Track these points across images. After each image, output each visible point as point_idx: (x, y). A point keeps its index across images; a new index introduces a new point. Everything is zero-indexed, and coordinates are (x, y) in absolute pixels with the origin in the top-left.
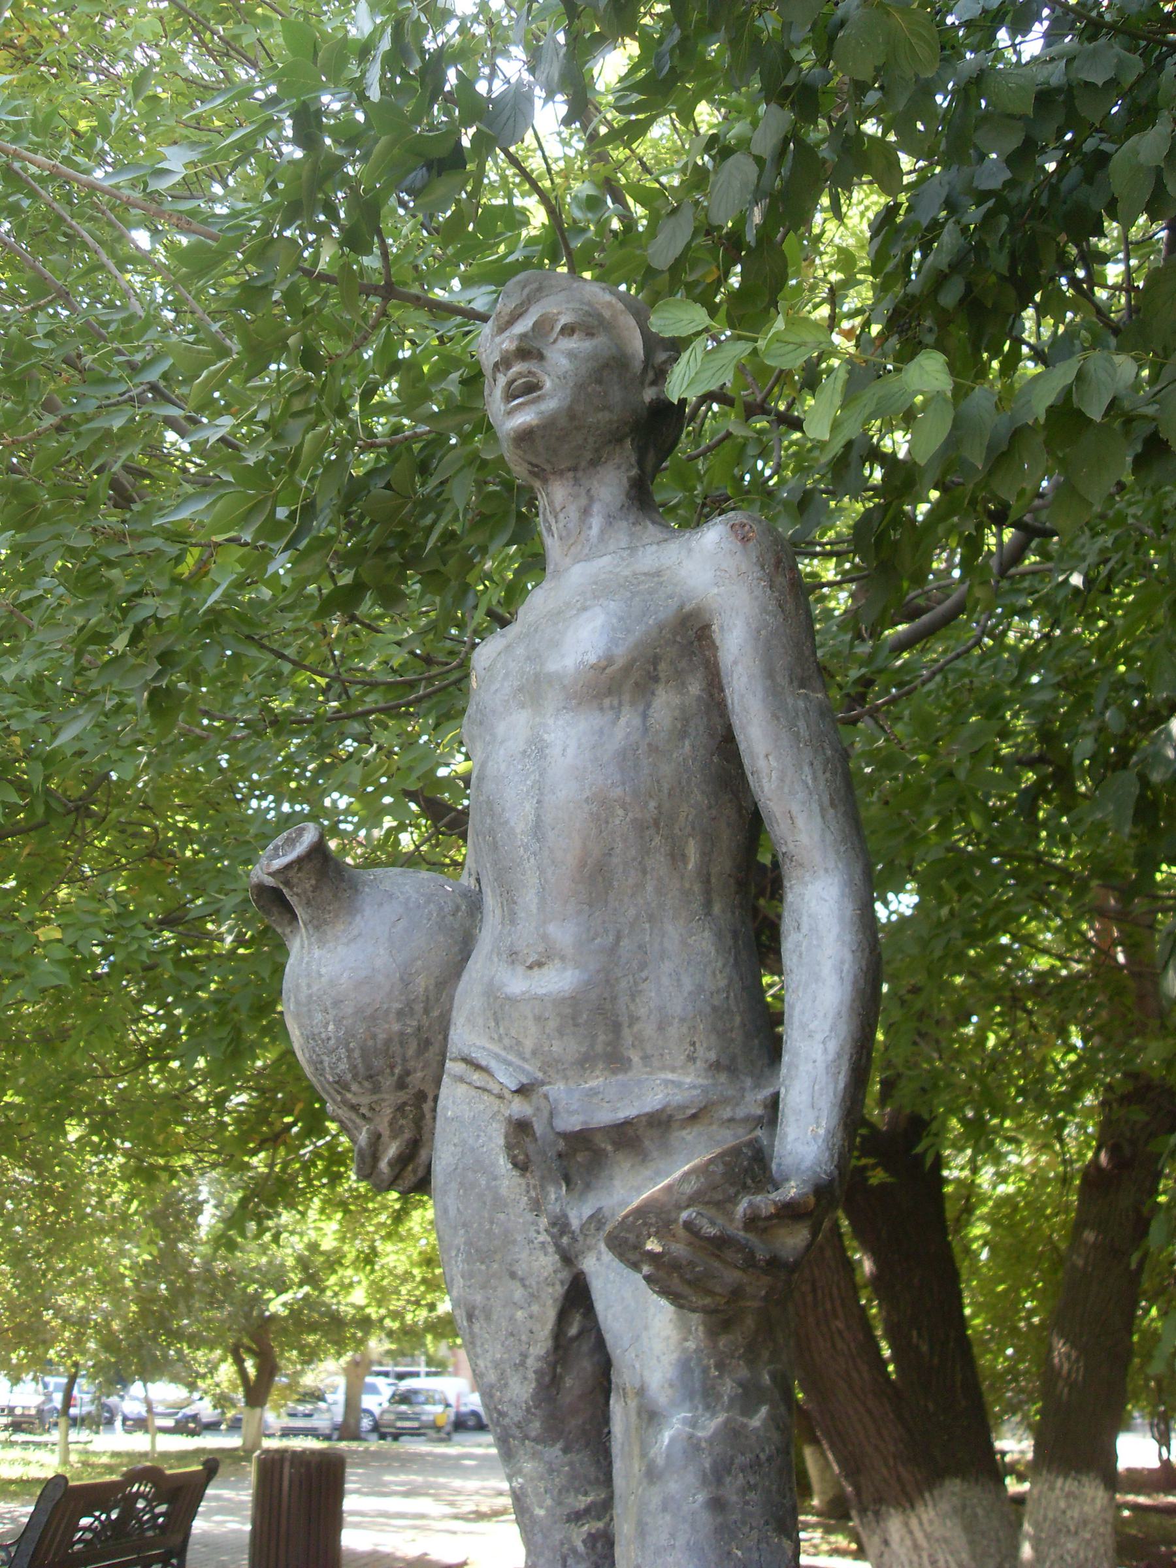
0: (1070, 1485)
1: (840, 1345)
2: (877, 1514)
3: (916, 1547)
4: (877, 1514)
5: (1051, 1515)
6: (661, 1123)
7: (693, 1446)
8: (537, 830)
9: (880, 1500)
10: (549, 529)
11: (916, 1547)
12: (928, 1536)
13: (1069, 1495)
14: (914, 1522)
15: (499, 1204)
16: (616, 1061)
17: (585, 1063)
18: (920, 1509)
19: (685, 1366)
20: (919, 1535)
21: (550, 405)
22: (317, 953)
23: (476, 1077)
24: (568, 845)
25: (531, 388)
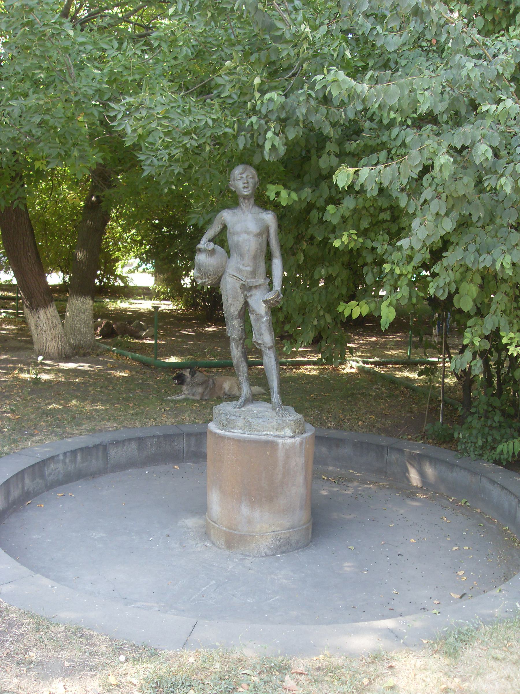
0: (83, 299)
1: (30, 260)
2: (37, 310)
3: (48, 318)
4: (37, 310)
5: (77, 308)
6: (260, 285)
7: (267, 320)
8: (248, 250)
9: (38, 306)
11: (48, 318)
12: (51, 316)
13: (83, 302)
14: (47, 312)
15: (237, 292)
16: (255, 278)
17: (251, 278)
18: (49, 308)
19: (266, 312)
20: (49, 315)
21: (250, 192)
24: (252, 253)
25: (247, 188)
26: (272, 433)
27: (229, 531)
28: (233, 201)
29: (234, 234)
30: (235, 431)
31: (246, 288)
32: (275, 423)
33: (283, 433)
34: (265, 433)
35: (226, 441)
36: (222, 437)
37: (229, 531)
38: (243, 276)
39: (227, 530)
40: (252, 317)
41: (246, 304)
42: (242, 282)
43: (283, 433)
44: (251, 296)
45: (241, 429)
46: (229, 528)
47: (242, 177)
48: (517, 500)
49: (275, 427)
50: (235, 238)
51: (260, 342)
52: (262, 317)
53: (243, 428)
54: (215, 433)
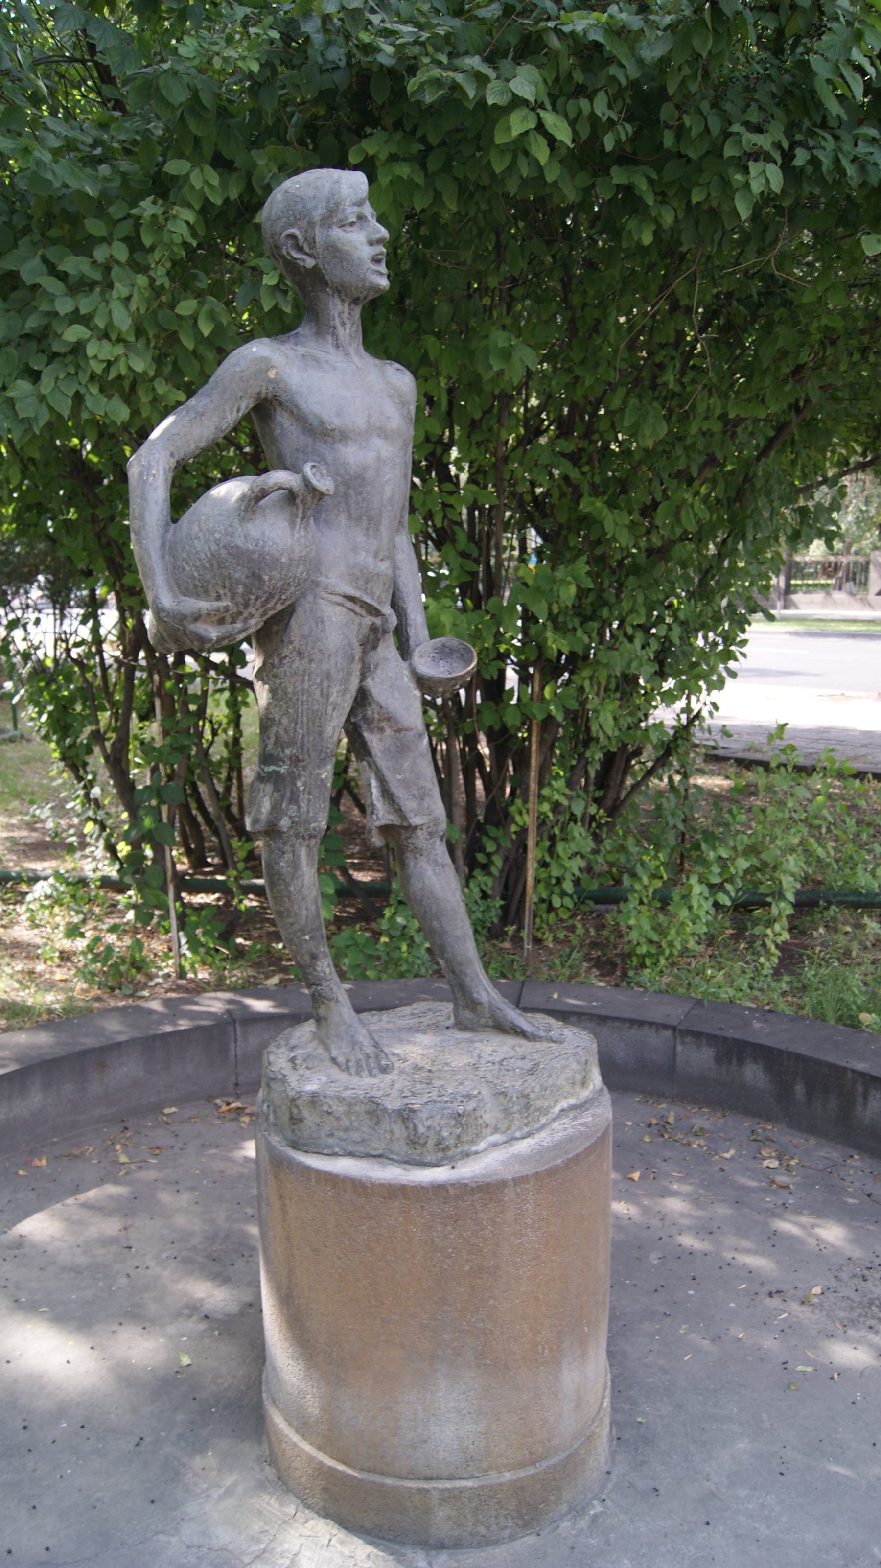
8: (391, 500)
10: (343, 324)
22: (303, 533)
23: (350, 604)
26: (572, 1101)
27: (531, 1471)
28: (299, 301)
29: (344, 436)
30: (482, 1145)
31: (371, 640)
32: (574, 1066)
33: (591, 1087)
34: (557, 1110)
35: (510, 1193)
36: (488, 1190)
37: (531, 1471)
38: (372, 595)
39: (522, 1474)
40: (373, 740)
41: (362, 697)
42: (369, 620)
43: (591, 1087)
44: (376, 667)
45: (496, 1130)
46: (522, 1465)
47: (361, 218)
48: (668, 1033)
49: (579, 1077)
50: (352, 455)
51: (416, 820)
52: (420, 736)
53: (503, 1127)
54: (439, 1188)
